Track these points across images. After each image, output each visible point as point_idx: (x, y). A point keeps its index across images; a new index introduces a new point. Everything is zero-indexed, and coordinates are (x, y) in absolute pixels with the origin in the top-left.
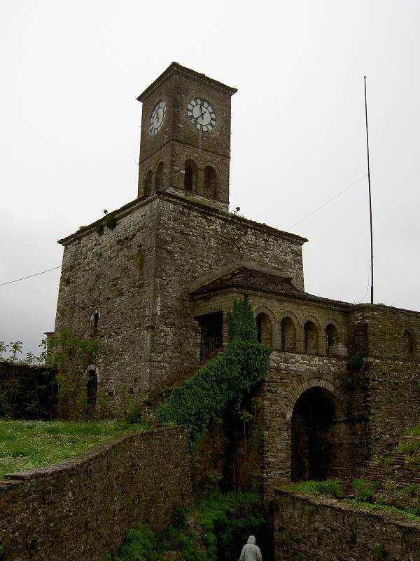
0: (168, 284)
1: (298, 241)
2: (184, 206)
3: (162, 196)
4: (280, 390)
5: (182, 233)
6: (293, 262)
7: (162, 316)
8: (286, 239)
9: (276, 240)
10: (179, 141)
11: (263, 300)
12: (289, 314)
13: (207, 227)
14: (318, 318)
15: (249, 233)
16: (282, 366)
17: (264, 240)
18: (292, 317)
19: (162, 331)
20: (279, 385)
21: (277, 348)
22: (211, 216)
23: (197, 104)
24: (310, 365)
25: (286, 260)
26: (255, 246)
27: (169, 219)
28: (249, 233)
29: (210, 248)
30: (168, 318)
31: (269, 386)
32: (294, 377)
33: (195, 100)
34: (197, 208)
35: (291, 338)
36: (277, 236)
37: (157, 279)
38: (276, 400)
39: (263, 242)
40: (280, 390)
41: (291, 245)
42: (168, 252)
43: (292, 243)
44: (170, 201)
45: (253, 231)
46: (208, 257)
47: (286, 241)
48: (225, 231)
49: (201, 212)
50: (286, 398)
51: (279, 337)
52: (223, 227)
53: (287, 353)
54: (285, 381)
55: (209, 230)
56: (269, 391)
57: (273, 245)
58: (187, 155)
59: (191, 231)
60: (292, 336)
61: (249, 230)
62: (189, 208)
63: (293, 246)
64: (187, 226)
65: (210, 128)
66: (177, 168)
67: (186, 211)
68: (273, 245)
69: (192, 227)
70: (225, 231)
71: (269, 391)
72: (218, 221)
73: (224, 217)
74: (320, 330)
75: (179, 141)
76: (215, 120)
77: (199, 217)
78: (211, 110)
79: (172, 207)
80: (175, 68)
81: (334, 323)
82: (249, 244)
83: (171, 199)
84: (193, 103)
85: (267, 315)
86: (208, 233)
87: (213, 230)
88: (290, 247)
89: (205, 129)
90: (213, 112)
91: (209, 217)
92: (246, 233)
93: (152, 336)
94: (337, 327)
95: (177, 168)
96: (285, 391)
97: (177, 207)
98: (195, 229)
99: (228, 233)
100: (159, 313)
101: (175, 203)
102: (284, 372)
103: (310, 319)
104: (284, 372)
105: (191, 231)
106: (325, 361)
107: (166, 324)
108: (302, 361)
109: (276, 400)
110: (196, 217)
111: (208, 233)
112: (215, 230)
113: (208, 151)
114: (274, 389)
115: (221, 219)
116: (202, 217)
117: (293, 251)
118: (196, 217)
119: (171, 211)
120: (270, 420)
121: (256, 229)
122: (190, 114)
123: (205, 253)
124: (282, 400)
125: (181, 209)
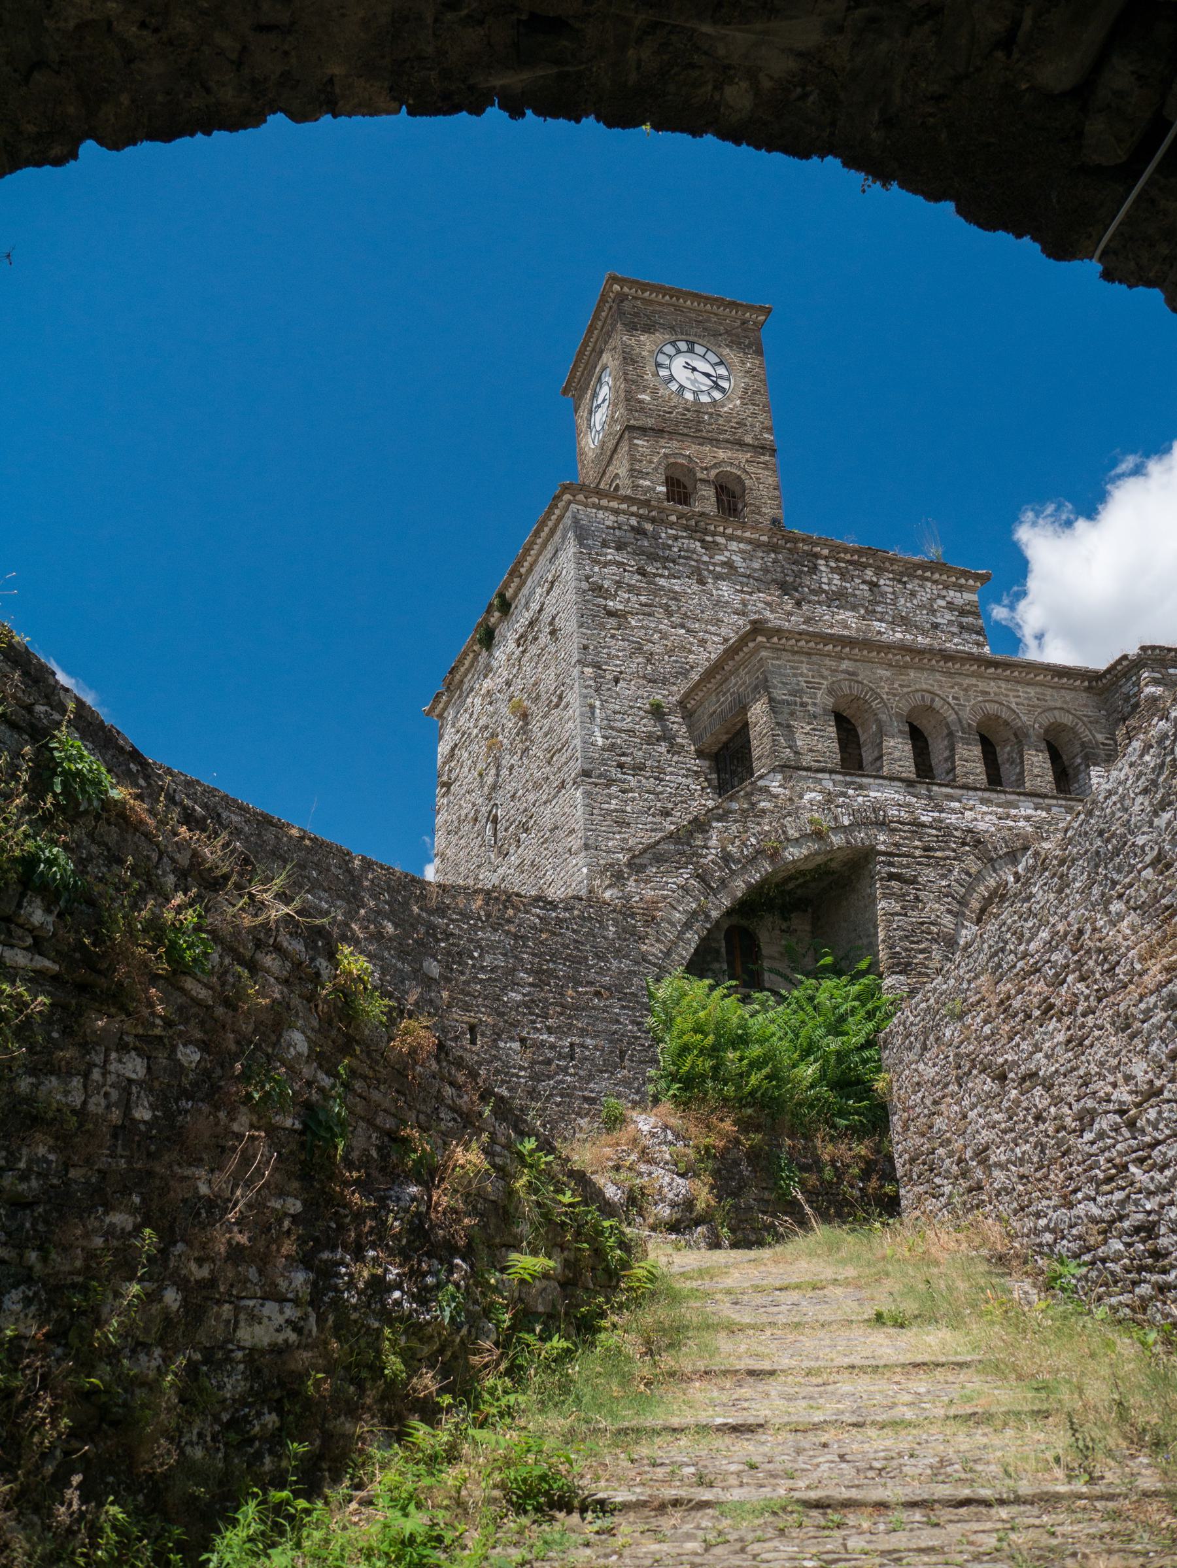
0: (617, 681)
1: (962, 581)
2: (640, 516)
3: (581, 497)
4: (928, 874)
5: (642, 572)
6: (955, 629)
8: (927, 579)
9: (899, 581)
11: (845, 665)
12: (927, 695)
13: (706, 558)
14: (1014, 706)
15: (823, 568)
16: (923, 819)
17: (864, 582)
18: (938, 703)
19: (611, 782)
20: (919, 863)
22: (714, 534)
23: (679, 351)
24: (1008, 817)
25: (936, 626)
27: (605, 544)
28: (823, 568)
29: (718, 604)
30: (624, 755)
31: (891, 864)
32: (964, 844)
33: (673, 343)
34: (673, 518)
35: (946, 760)
36: (902, 574)
37: (588, 671)
39: (865, 587)
41: (944, 593)
42: (611, 614)
43: (946, 588)
44: (606, 509)
45: (833, 564)
46: (718, 622)
47: (929, 584)
48: (756, 565)
49: (686, 528)
52: (747, 556)
53: (935, 788)
54: (939, 854)
55: (715, 565)
56: (891, 877)
57: (894, 593)
58: (666, 456)
59: (665, 568)
60: (947, 754)
61: (822, 562)
62: (653, 521)
63: (951, 593)
64: (652, 557)
65: (717, 395)
66: (647, 483)
67: (649, 527)
68: (894, 593)
69: (667, 559)
70: (756, 565)
71: (891, 877)
72: (734, 546)
73: (747, 534)
74: (1027, 735)
78: (715, 360)
79: (610, 520)
80: (617, 287)
81: (1067, 719)
82: (824, 591)
83: (604, 502)
84: (669, 349)
86: (710, 572)
87: (723, 564)
88: (939, 596)
89: (704, 399)
90: (721, 363)
91: (709, 539)
92: (814, 569)
93: (588, 794)
94: (1081, 728)
95: (647, 483)
96: (944, 877)
97: (622, 518)
98: (674, 562)
99: (766, 571)
100: (600, 741)
101: (616, 512)
103: (992, 708)
104: (934, 832)
106: (1055, 810)
107: (621, 766)
109: (917, 898)
110: (676, 538)
111: (710, 572)
112: (729, 564)
115: (740, 540)
116: (691, 538)
117: (951, 606)
118: (676, 538)
119: (608, 527)
120: (906, 950)
121: (837, 560)
122: (663, 373)
124: (938, 900)
125: (634, 521)
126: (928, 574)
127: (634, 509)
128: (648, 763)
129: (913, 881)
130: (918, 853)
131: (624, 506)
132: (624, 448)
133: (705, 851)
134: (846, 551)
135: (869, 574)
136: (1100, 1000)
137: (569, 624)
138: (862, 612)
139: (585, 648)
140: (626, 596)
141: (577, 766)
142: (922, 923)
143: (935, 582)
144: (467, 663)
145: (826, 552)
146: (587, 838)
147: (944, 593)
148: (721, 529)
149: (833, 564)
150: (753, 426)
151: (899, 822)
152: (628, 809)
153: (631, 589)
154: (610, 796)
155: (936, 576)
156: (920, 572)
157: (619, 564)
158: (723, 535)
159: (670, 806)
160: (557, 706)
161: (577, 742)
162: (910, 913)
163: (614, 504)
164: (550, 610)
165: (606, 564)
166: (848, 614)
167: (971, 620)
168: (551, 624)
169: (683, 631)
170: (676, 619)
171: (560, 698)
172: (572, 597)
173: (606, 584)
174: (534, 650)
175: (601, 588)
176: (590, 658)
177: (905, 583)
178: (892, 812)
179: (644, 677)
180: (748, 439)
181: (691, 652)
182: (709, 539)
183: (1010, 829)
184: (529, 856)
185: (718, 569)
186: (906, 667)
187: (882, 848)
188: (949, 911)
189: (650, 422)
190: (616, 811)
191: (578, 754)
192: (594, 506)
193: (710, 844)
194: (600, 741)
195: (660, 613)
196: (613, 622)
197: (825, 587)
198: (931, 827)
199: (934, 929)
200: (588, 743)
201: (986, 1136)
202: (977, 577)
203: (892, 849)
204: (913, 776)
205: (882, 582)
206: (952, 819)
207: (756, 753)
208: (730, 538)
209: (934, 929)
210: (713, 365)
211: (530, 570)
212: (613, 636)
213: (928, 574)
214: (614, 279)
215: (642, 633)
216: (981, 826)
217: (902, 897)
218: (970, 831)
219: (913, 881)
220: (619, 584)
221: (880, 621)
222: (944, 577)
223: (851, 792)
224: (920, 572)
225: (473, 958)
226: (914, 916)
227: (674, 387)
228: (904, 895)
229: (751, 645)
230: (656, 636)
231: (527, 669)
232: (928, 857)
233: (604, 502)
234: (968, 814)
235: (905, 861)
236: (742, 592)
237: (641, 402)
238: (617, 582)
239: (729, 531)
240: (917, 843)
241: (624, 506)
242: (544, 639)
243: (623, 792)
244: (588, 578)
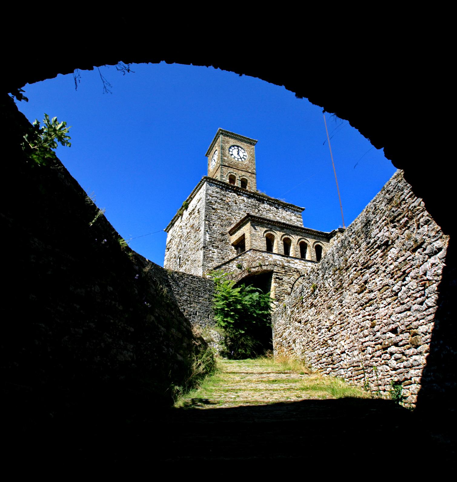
0: (213, 225)
1: (298, 210)
4: (285, 278)
5: (221, 199)
6: (296, 221)
7: (211, 242)
10: (225, 166)
19: (210, 250)
21: (281, 254)
22: (240, 192)
23: (235, 149)
25: (291, 220)
26: (269, 210)
27: (213, 192)
28: (266, 203)
29: (240, 209)
30: (214, 244)
31: (277, 275)
34: (230, 187)
36: (284, 207)
37: (207, 222)
38: (282, 284)
40: (285, 278)
41: (294, 212)
42: (213, 209)
45: (268, 202)
47: (290, 210)
49: (233, 190)
50: (290, 283)
51: (283, 248)
63: (295, 212)
66: (225, 179)
69: (228, 197)
75: (225, 166)
76: (246, 156)
77: (232, 192)
80: (221, 132)
82: (266, 209)
83: (214, 182)
85: (272, 234)
86: (238, 201)
91: (239, 193)
96: (289, 279)
98: (230, 198)
102: (287, 268)
104: (287, 268)
105: (227, 199)
107: (213, 246)
108: (300, 264)
109: (282, 284)
111: (238, 201)
113: (242, 171)
114: (280, 277)
120: (279, 296)
122: (230, 153)
123: (237, 211)
126: (290, 207)
127: (221, 184)
128: (219, 246)
129: (282, 279)
130: (283, 273)
131: (219, 183)
132: (219, 170)
133: (232, 268)
134: (271, 199)
135: (276, 205)
136: (324, 302)
137: (203, 211)
138: (274, 214)
139: (206, 216)
140: (217, 205)
141: (202, 245)
142: (283, 290)
143: (292, 209)
144: (176, 219)
145: (266, 199)
146: (203, 263)
147: (294, 212)
148: (242, 191)
149: (268, 202)
150: (251, 168)
151: (279, 265)
152: (214, 257)
153: (219, 203)
154: (209, 253)
155: (292, 208)
156: (288, 206)
157: (216, 197)
158: (242, 193)
159: (224, 257)
160: (198, 230)
161: (202, 240)
162: (280, 287)
163: (216, 183)
164: (198, 207)
165: (213, 197)
166: (271, 214)
167: (299, 219)
168: (198, 210)
169: (231, 215)
170: (229, 211)
171: (199, 228)
172: (204, 204)
173: (212, 201)
174: (193, 216)
175: (211, 202)
176: (208, 218)
177: (285, 209)
178: (278, 262)
179: (220, 225)
180: (250, 171)
181: (232, 220)
182: (239, 193)
183: (305, 269)
184: (188, 267)
185: (240, 201)
186: (284, 228)
187: (275, 271)
188: (290, 287)
189: (227, 164)
190: (211, 257)
191: (202, 243)
192: (211, 182)
193: (233, 266)
194: (208, 240)
195: (225, 210)
196: (213, 211)
197: (266, 208)
198: (287, 267)
199: (286, 291)
200: (205, 240)
201: (295, 336)
202: (302, 209)
203: (278, 271)
204: (284, 254)
205: (279, 208)
206: (292, 265)
207: (246, 245)
208: (244, 193)
209: (286, 291)
210: (243, 153)
211: (194, 197)
212: (213, 214)
213: (290, 207)
214: (220, 130)
215: (220, 214)
216: (298, 268)
217: (279, 283)
218: (296, 268)
219: (282, 279)
220: (216, 202)
221: (279, 217)
222: (294, 208)
223: (269, 257)
224: (288, 206)
225: (173, 288)
226: (282, 288)
227: (233, 156)
228: (279, 283)
229: (247, 219)
230: (224, 215)
231: (191, 220)
232: (286, 274)
233: (214, 182)
234: (296, 265)
235: (280, 274)
236: (245, 207)
237: (225, 159)
238: (215, 201)
239: (244, 192)
240: (283, 270)
241: (219, 183)
242: (196, 214)
243: (213, 253)
244: (208, 200)
